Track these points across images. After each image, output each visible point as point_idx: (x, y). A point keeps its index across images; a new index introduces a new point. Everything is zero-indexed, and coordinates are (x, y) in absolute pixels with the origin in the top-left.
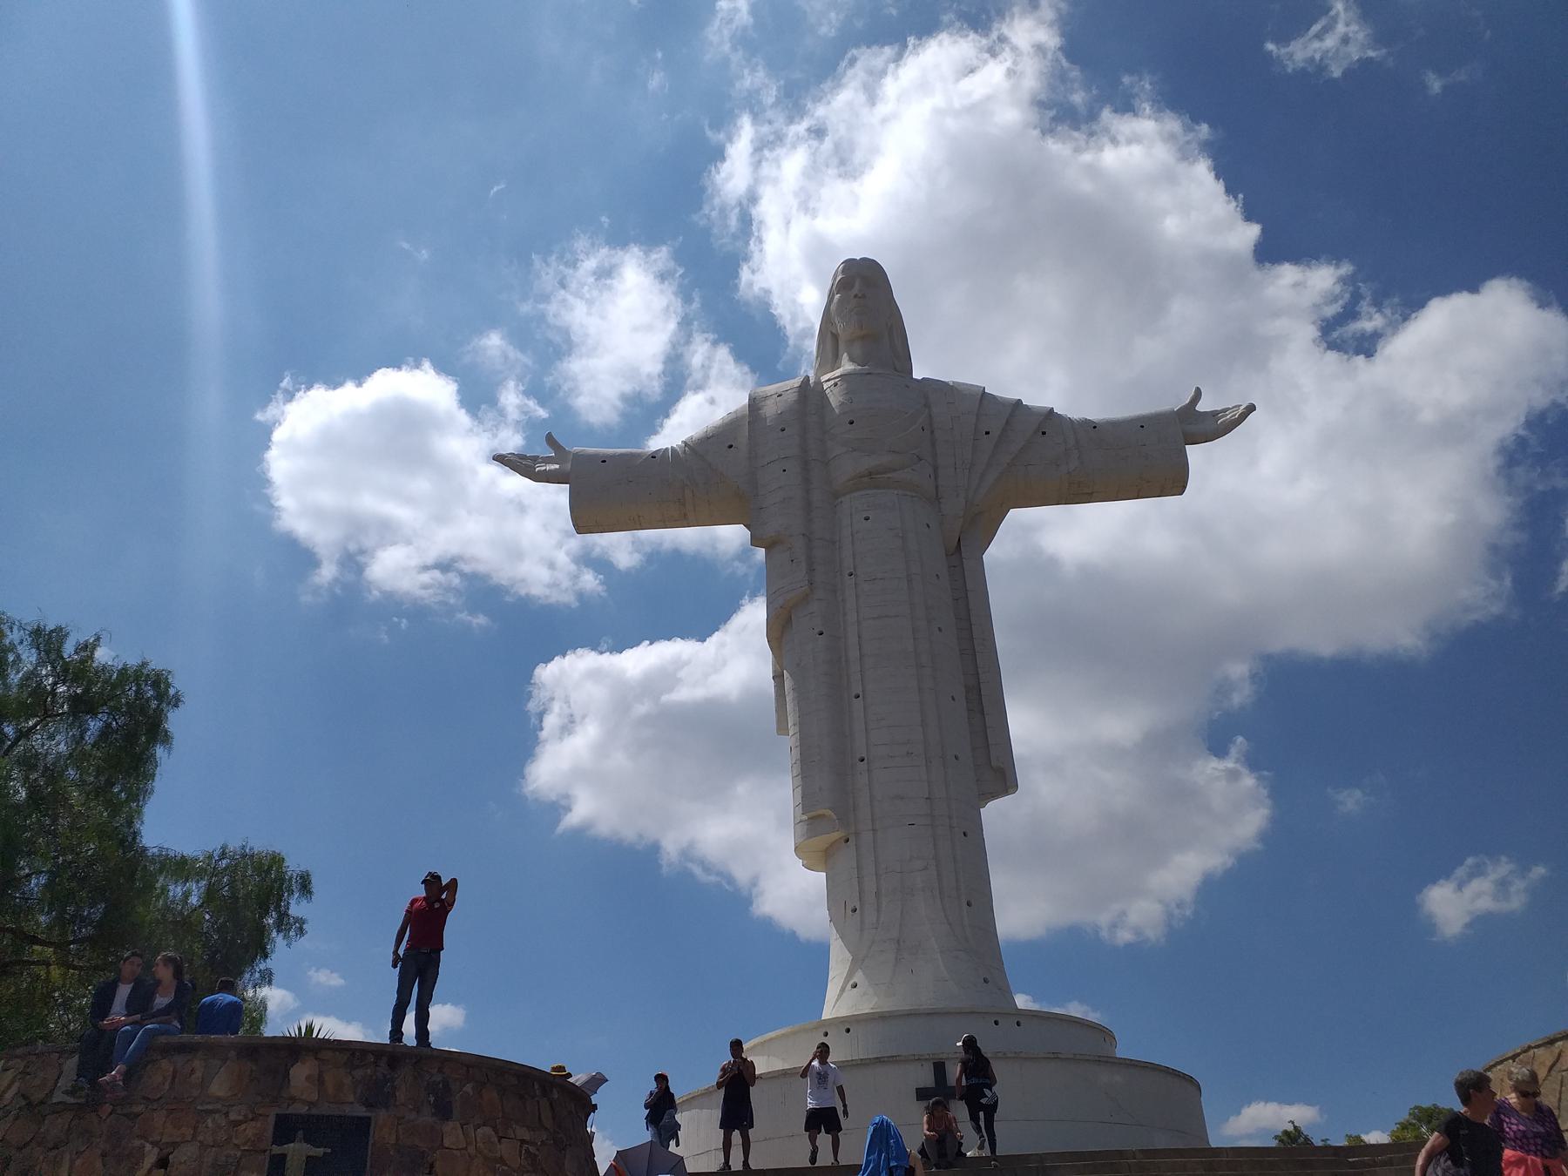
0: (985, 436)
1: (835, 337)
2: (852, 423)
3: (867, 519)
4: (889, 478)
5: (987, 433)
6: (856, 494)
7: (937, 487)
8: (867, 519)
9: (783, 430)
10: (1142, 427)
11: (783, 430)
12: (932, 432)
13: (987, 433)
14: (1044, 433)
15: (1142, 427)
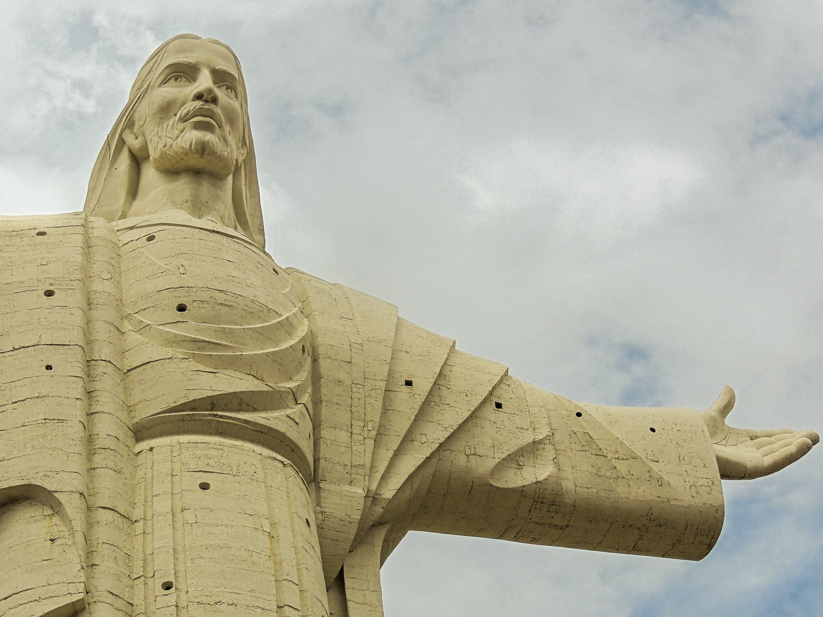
0: (406, 388)
1: (138, 160)
2: (182, 308)
3: (204, 486)
4: (246, 422)
5: (409, 383)
6: (184, 438)
7: (316, 461)
8: (204, 486)
9: (49, 294)
10: (653, 430)
11: (49, 294)
12: (315, 361)
13: (409, 383)
14: (499, 406)
15: (653, 430)
